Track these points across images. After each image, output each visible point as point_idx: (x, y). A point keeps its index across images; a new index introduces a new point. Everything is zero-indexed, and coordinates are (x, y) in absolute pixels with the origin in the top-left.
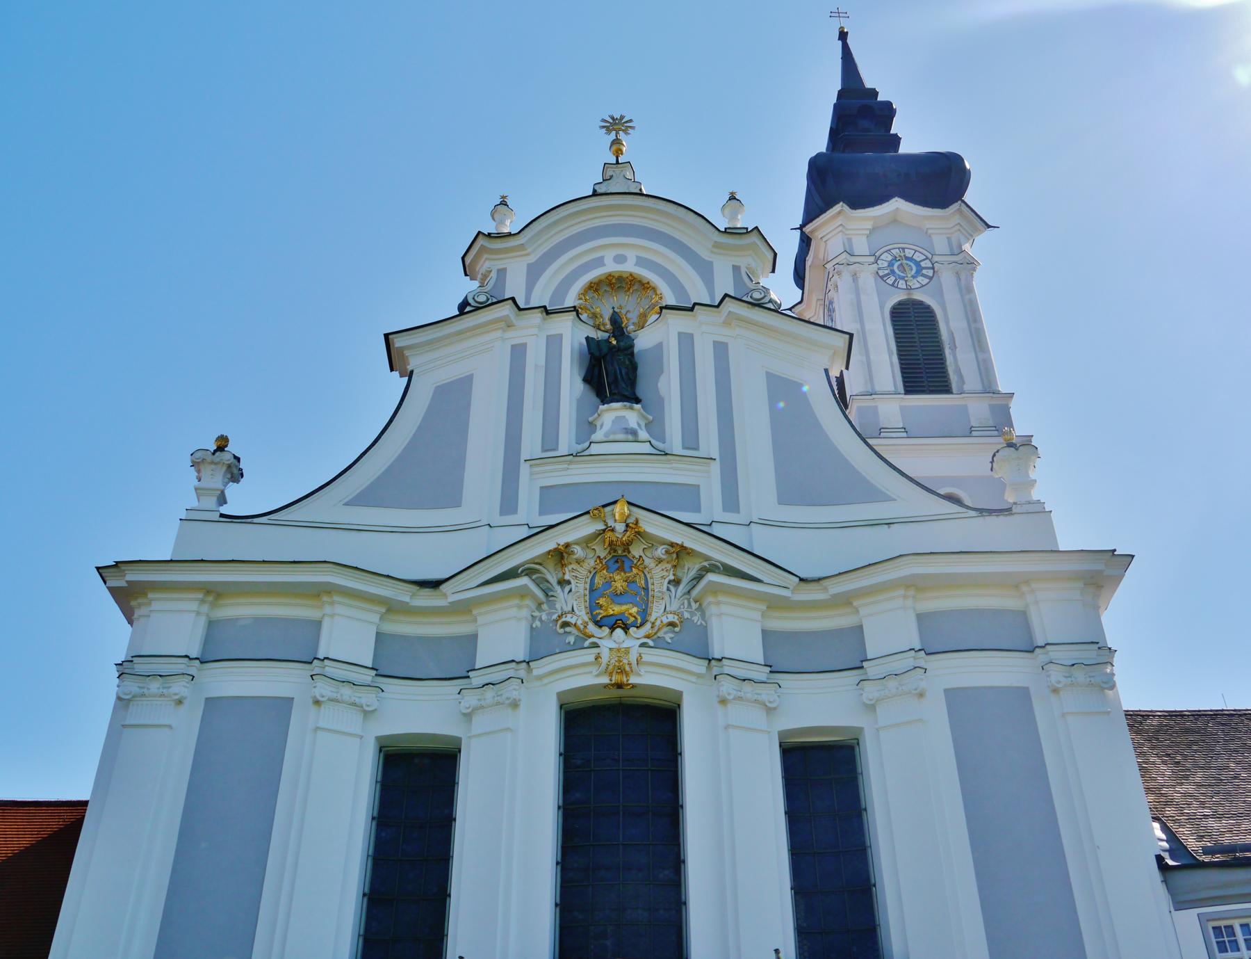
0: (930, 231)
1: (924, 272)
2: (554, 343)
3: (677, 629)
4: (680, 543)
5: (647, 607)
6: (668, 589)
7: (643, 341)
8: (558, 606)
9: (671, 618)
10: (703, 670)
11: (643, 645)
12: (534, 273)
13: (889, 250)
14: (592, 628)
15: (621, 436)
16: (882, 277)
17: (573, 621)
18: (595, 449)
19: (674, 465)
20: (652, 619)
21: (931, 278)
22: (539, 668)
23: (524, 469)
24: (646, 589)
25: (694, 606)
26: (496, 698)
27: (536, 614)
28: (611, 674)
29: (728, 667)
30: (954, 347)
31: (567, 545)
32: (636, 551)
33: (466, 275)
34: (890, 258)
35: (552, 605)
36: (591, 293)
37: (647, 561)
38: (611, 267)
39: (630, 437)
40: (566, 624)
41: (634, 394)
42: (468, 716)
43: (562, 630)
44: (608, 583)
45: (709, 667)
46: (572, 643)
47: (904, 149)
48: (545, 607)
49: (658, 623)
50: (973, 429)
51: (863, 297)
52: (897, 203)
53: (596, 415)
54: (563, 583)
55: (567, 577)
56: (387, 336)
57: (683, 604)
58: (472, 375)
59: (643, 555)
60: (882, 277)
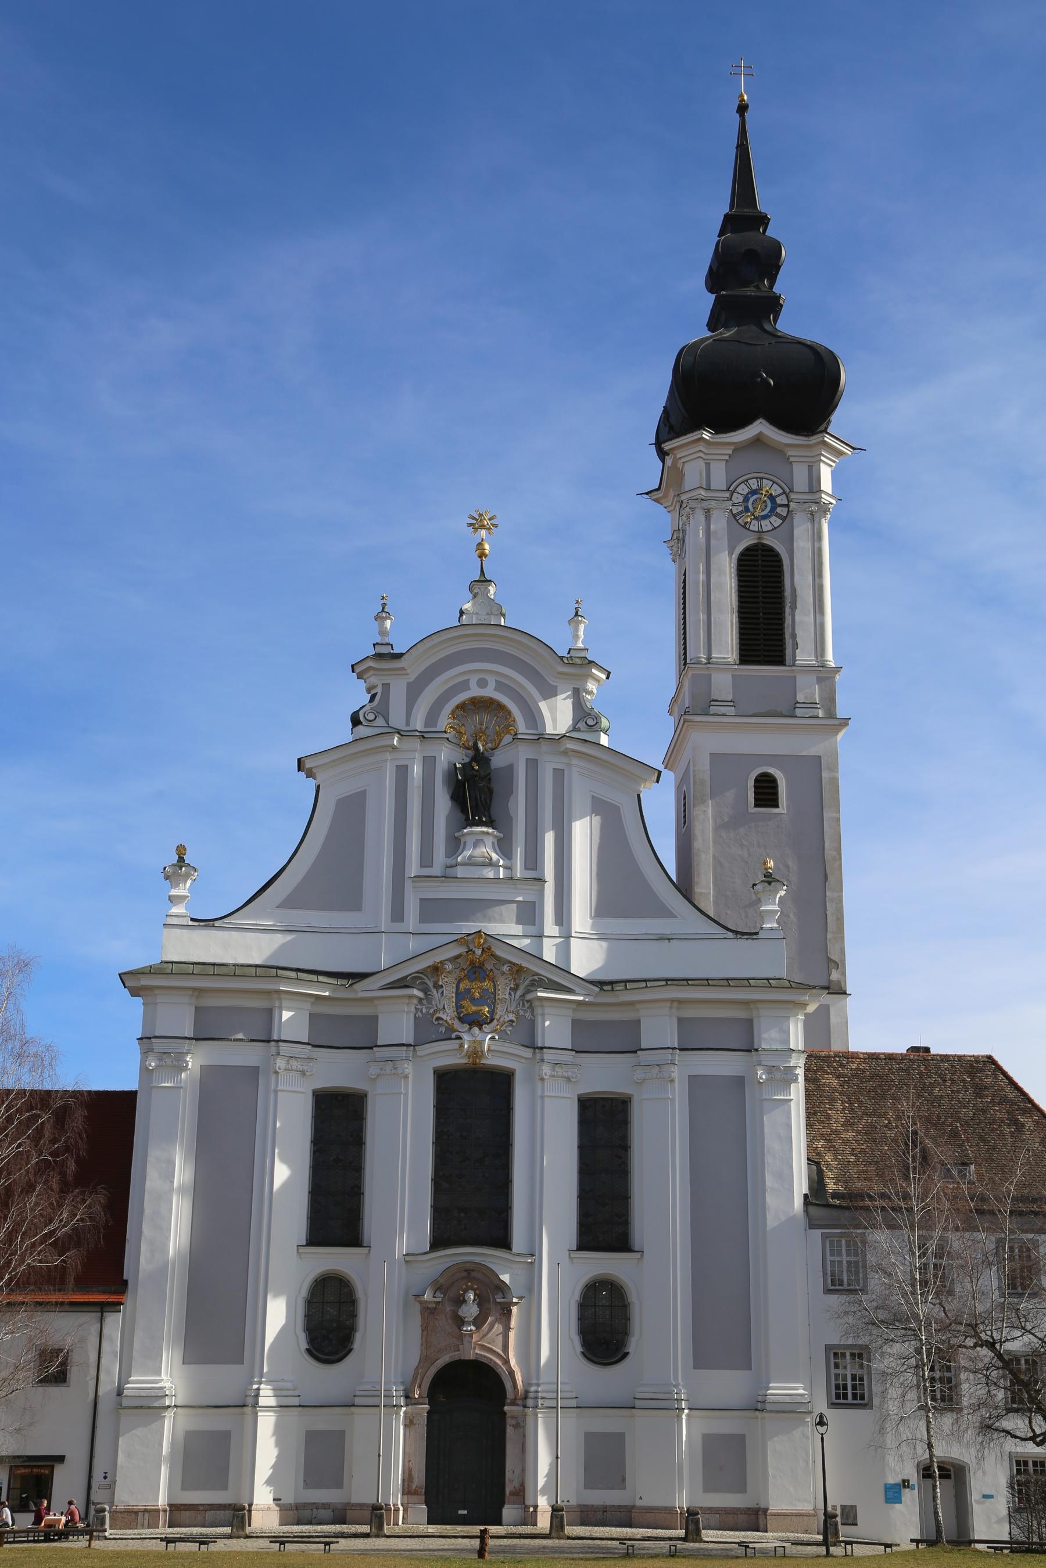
0: (791, 459)
1: (779, 510)
2: (429, 763)
3: (514, 1024)
4: (518, 962)
5: (494, 1008)
6: (510, 994)
7: (498, 760)
8: (434, 1003)
9: (512, 1017)
12: (414, 691)
13: (747, 481)
14: (457, 1024)
16: (734, 516)
17: (444, 1017)
18: (460, 872)
19: (518, 886)
20: (497, 1017)
22: (422, 1050)
23: (408, 885)
24: (494, 994)
25: (527, 1005)
26: (393, 1071)
27: (419, 1007)
28: (469, 1058)
29: (548, 1055)
30: (794, 608)
31: (441, 962)
32: (488, 966)
33: (353, 671)
34: (746, 491)
35: (430, 1001)
36: (458, 712)
37: (496, 972)
40: (439, 1019)
41: (490, 817)
42: (373, 1080)
43: (437, 1022)
44: (468, 991)
45: (534, 1053)
46: (443, 1032)
47: (787, 324)
48: (425, 1002)
49: (502, 1020)
50: (798, 705)
51: (713, 542)
52: (761, 424)
53: (460, 833)
54: (437, 986)
55: (440, 983)
56: (299, 760)
57: (519, 1004)
58: (365, 790)
59: (493, 969)
60: (734, 516)
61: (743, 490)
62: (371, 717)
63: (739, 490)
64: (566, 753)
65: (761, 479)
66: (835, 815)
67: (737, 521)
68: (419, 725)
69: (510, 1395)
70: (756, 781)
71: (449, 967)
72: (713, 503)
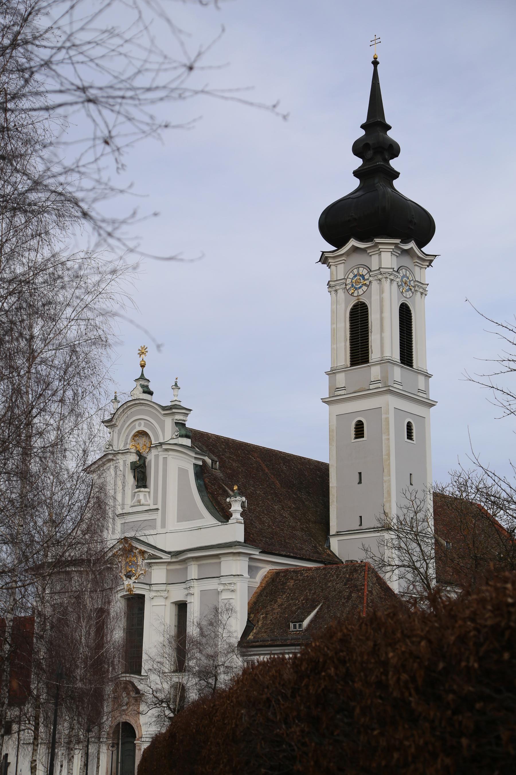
0: (370, 254)
6: (142, 562)
10: (149, 588)
11: (135, 582)
13: (353, 271)
15: (136, 504)
19: (149, 513)
21: (368, 286)
34: (353, 276)
38: (138, 429)
39: (139, 504)
45: (150, 587)
60: (347, 290)
61: (351, 276)
62: (107, 447)
63: (349, 277)
64: (166, 450)
65: (359, 268)
66: (387, 437)
67: (349, 293)
68: (121, 447)
69: (137, 737)
70: (356, 425)
71: (120, 553)
72: (338, 287)
